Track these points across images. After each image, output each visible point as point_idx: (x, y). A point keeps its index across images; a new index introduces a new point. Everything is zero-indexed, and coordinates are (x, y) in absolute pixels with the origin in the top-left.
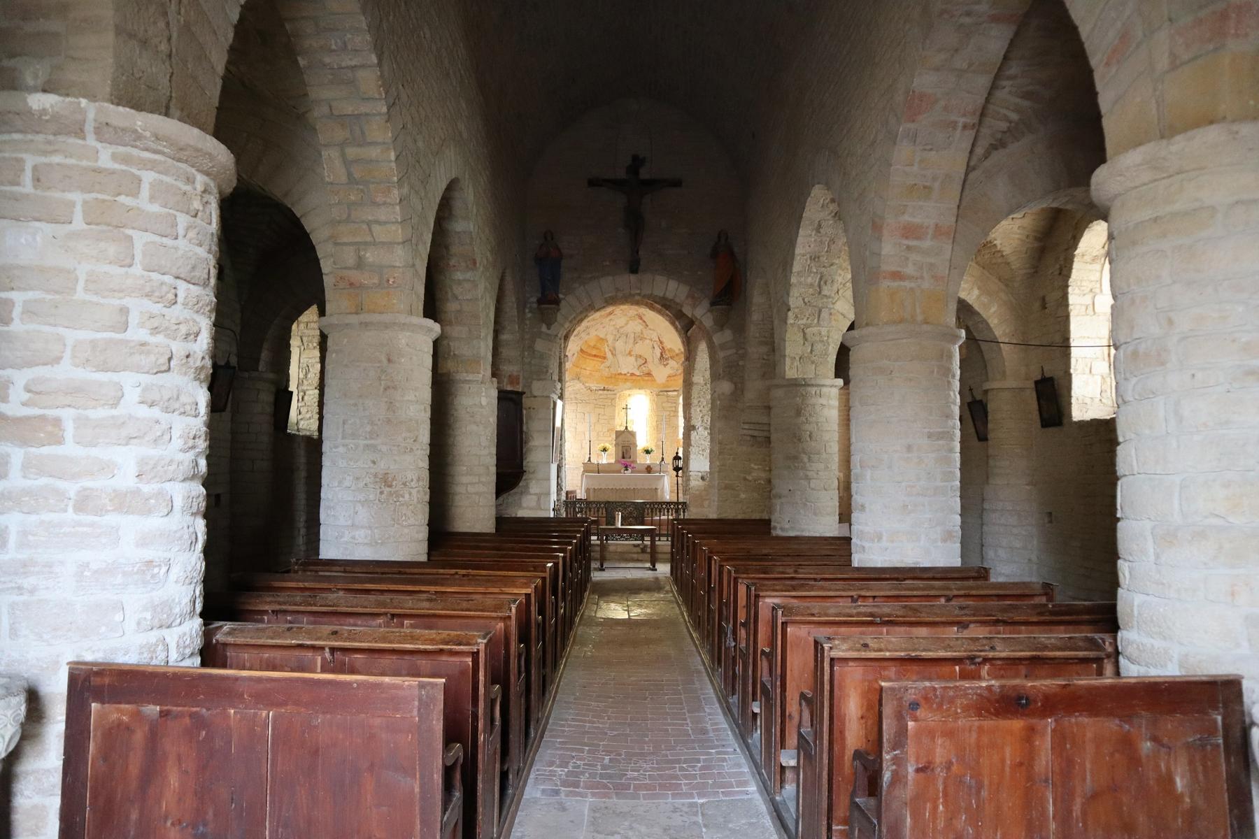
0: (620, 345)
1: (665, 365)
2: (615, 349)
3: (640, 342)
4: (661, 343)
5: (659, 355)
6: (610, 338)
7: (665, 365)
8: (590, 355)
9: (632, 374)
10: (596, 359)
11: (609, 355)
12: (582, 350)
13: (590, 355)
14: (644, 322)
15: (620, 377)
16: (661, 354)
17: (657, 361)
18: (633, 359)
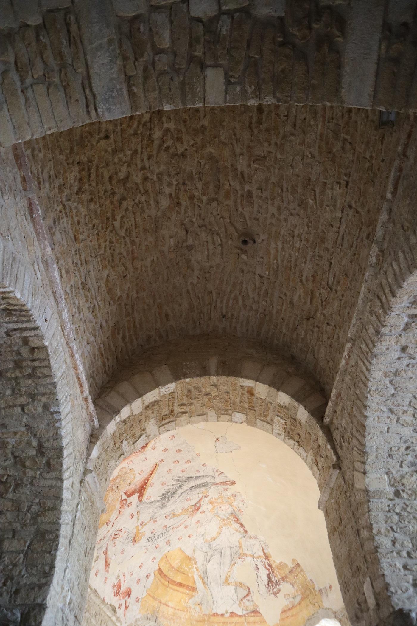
0: (213, 568)
1: (276, 594)
2: (206, 573)
3: (239, 561)
4: (267, 558)
5: (267, 578)
6: (199, 557)
7: (276, 594)
8: (174, 583)
9: (233, 614)
10: (181, 589)
11: (199, 584)
12: (160, 570)
13: (174, 583)
14: (242, 525)
15: (216, 619)
16: (269, 578)
17: (263, 589)
18: (232, 588)
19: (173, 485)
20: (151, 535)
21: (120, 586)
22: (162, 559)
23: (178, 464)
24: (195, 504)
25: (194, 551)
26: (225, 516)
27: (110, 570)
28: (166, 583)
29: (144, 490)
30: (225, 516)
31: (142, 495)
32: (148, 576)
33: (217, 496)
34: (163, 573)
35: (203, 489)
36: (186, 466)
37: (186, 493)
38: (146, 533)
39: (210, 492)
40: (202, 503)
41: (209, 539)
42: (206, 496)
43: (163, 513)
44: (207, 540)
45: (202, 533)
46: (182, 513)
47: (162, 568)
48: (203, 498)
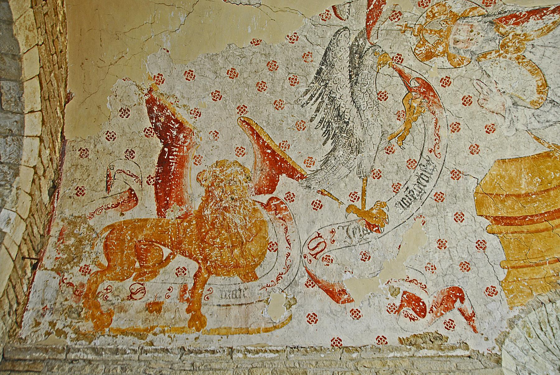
12: (497, 220)
19: (318, 110)
20: (402, 193)
21: (418, 300)
22: (479, 205)
23: (269, 85)
24: (409, 89)
25: (537, 139)
26: (494, 39)
27: (353, 296)
28: (541, 226)
29: (286, 162)
30: (494, 39)
31: (294, 169)
32: (481, 245)
33: (414, 40)
34: (515, 218)
35: (369, 60)
36: (281, 72)
37: (357, 93)
38: (384, 200)
39: (388, 50)
40: (415, 75)
41: (536, 97)
42: (400, 59)
43: (373, 153)
44: (532, 103)
45: (509, 103)
46: (408, 123)
47: (502, 213)
48: (401, 67)
